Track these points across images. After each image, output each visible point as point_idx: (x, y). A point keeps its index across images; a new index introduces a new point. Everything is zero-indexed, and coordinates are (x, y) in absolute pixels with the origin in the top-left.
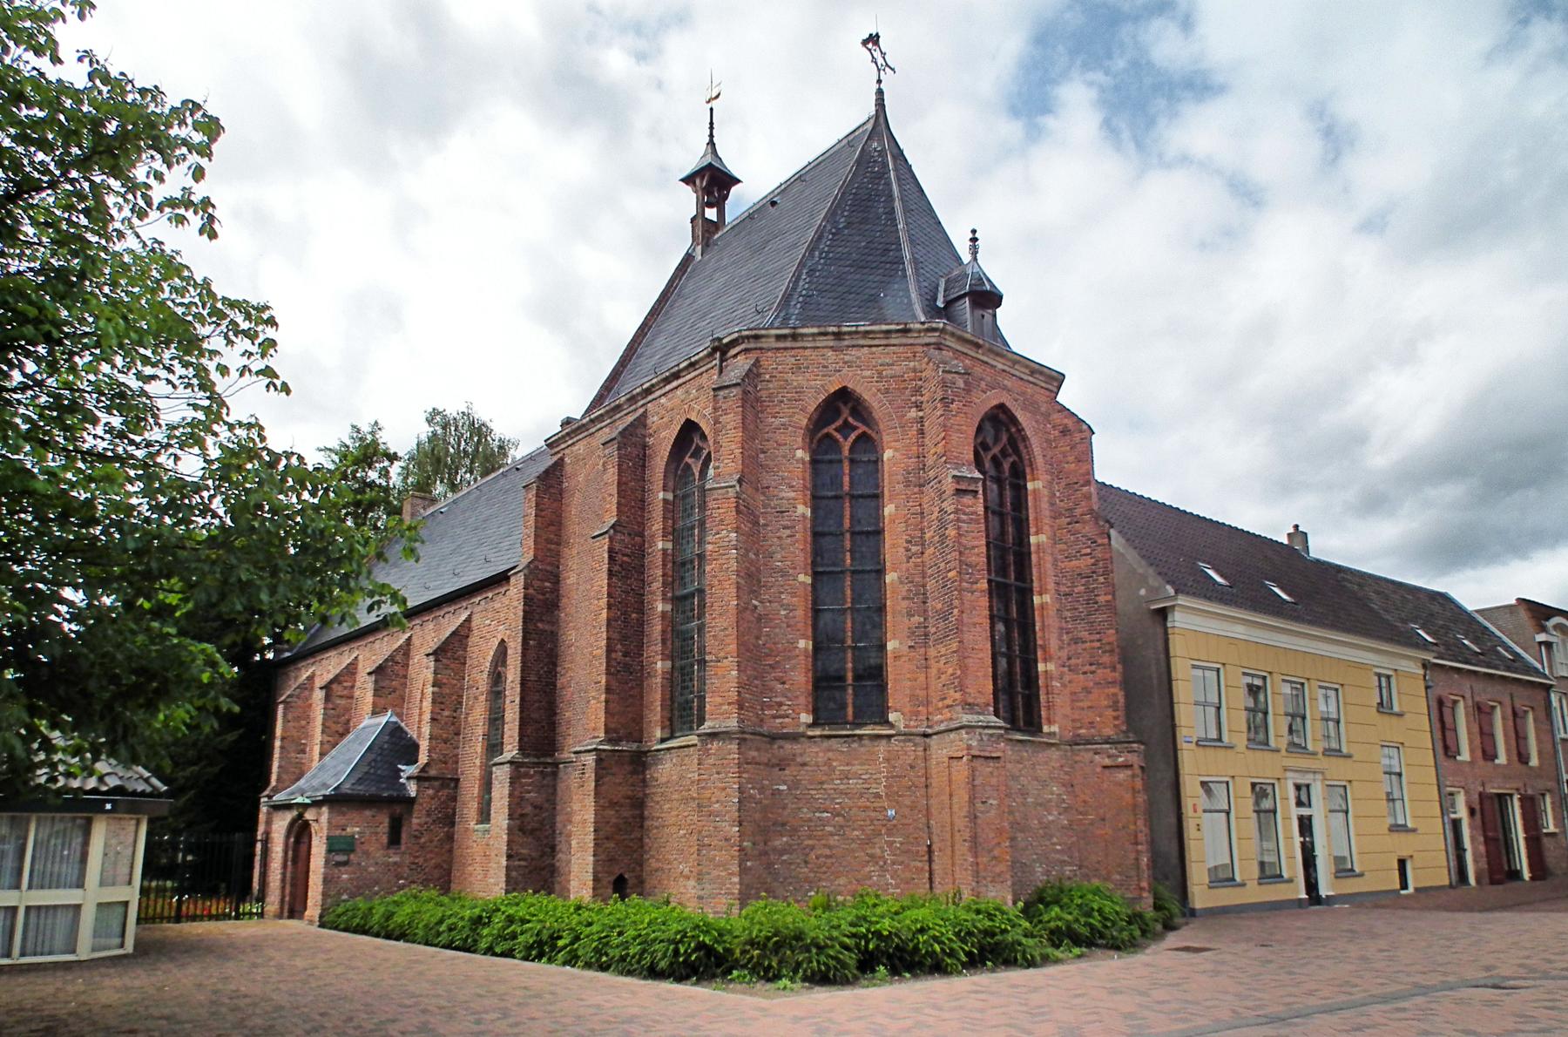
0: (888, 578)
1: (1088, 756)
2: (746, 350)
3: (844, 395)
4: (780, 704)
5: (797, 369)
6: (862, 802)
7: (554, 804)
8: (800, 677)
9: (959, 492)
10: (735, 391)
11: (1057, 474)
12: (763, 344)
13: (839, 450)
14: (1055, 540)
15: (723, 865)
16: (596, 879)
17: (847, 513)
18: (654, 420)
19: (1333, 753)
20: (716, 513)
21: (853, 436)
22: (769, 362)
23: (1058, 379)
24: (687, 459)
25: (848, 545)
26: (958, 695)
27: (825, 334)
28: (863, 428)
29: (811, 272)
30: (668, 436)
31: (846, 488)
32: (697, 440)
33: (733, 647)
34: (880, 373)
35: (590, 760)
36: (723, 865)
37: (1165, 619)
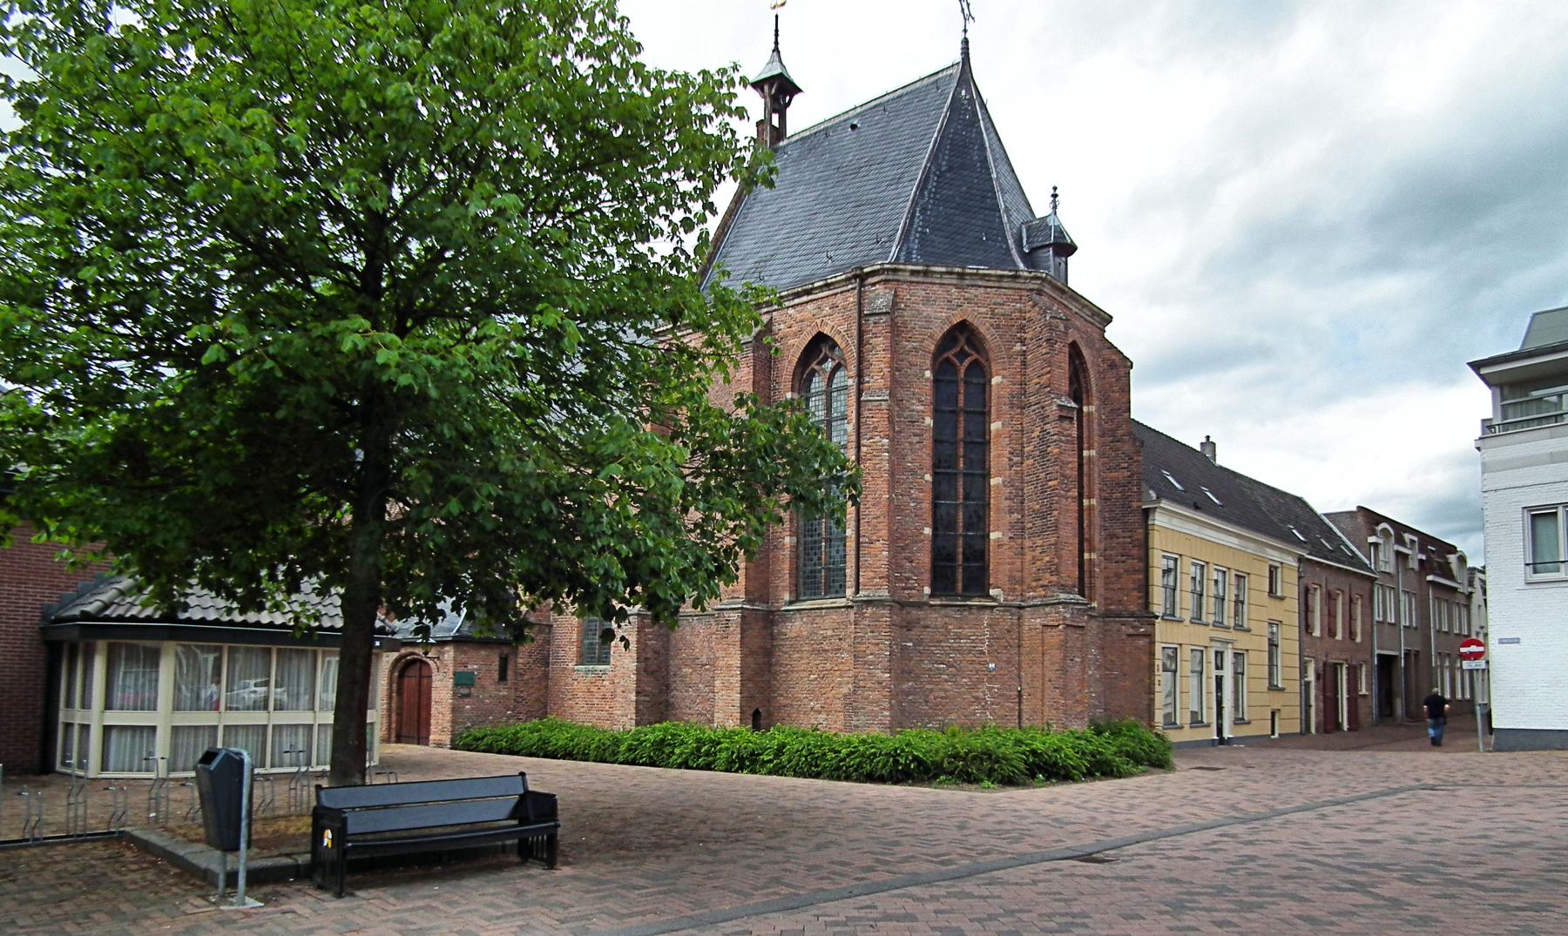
0: (993, 482)
1: (1117, 626)
2: (886, 281)
3: (963, 326)
4: (909, 579)
5: (926, 301)
6: (970, 657)
7: (667, 650)
8: (925, 558)
9: (1062, 418)
10: (884, 318)
11: (1105, 401)
12: (901, 276)
13: (956, 371)
14: (1101, 455)
15: (876, 702)
16: (742, 712)
17: (962, 425)
18: (781, 328)
19: (1239, 627)
20: (869, 421)
21: (967, 362)
22: (904, 292)
23: (1108, 319)
24: (814, 365)
25: (961, 451)
26: (1054, 578)
27: (951, 273)
28: (975, 356)
29: (924, 210)
30: (797, 344)
31: (961, 404)
32: (825, 350)
33: (884, 533)
34: (993, 310)
35: (735, 617)
36: (876, 702)
37: (1147, 518)
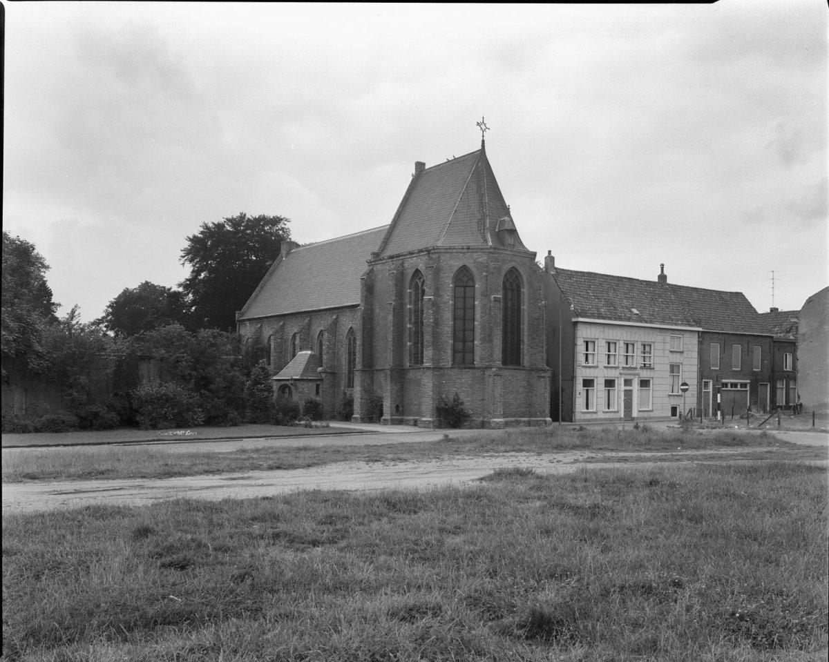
9: (495, 301)
